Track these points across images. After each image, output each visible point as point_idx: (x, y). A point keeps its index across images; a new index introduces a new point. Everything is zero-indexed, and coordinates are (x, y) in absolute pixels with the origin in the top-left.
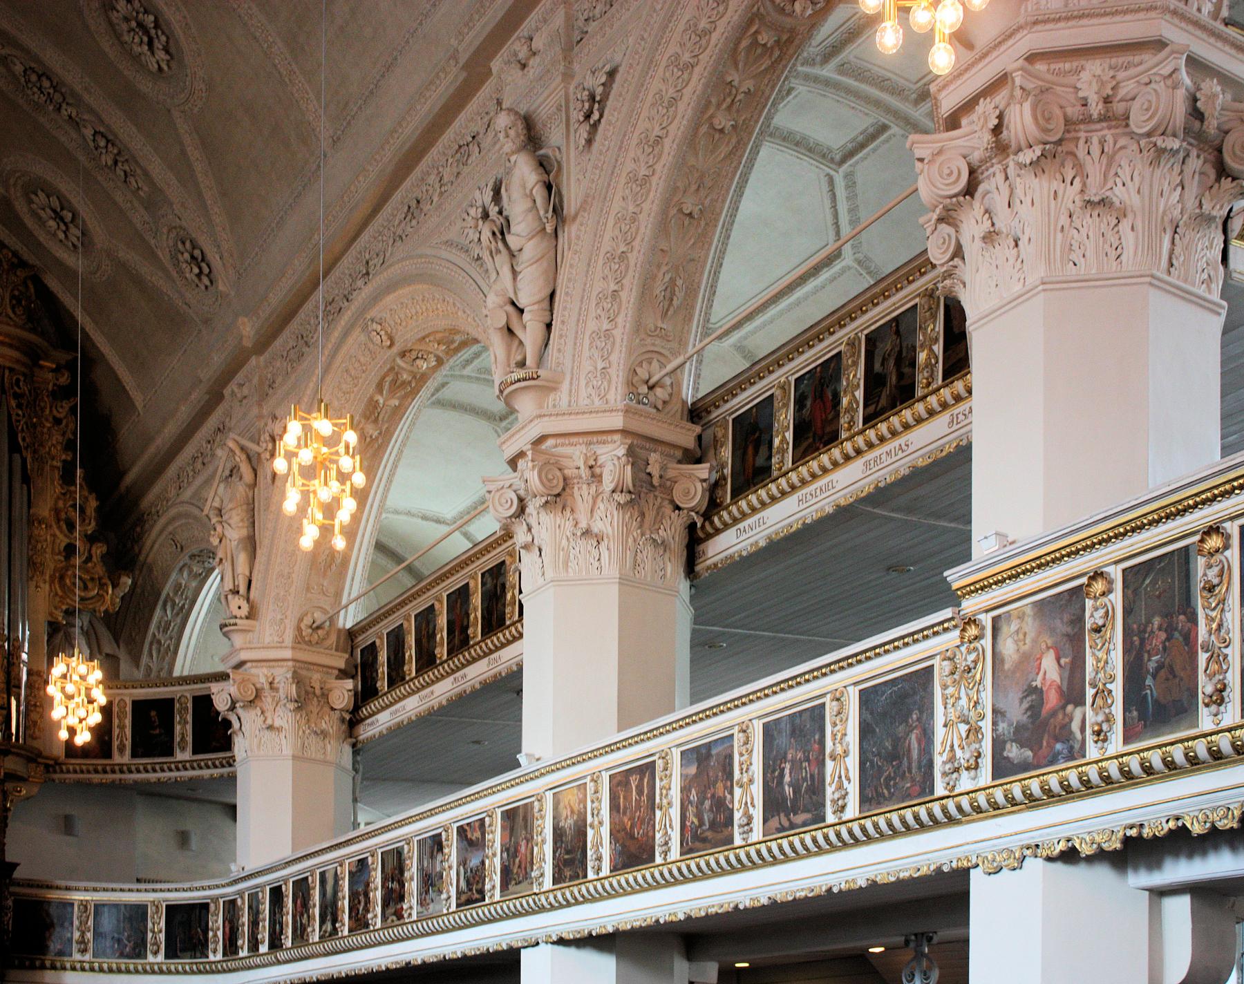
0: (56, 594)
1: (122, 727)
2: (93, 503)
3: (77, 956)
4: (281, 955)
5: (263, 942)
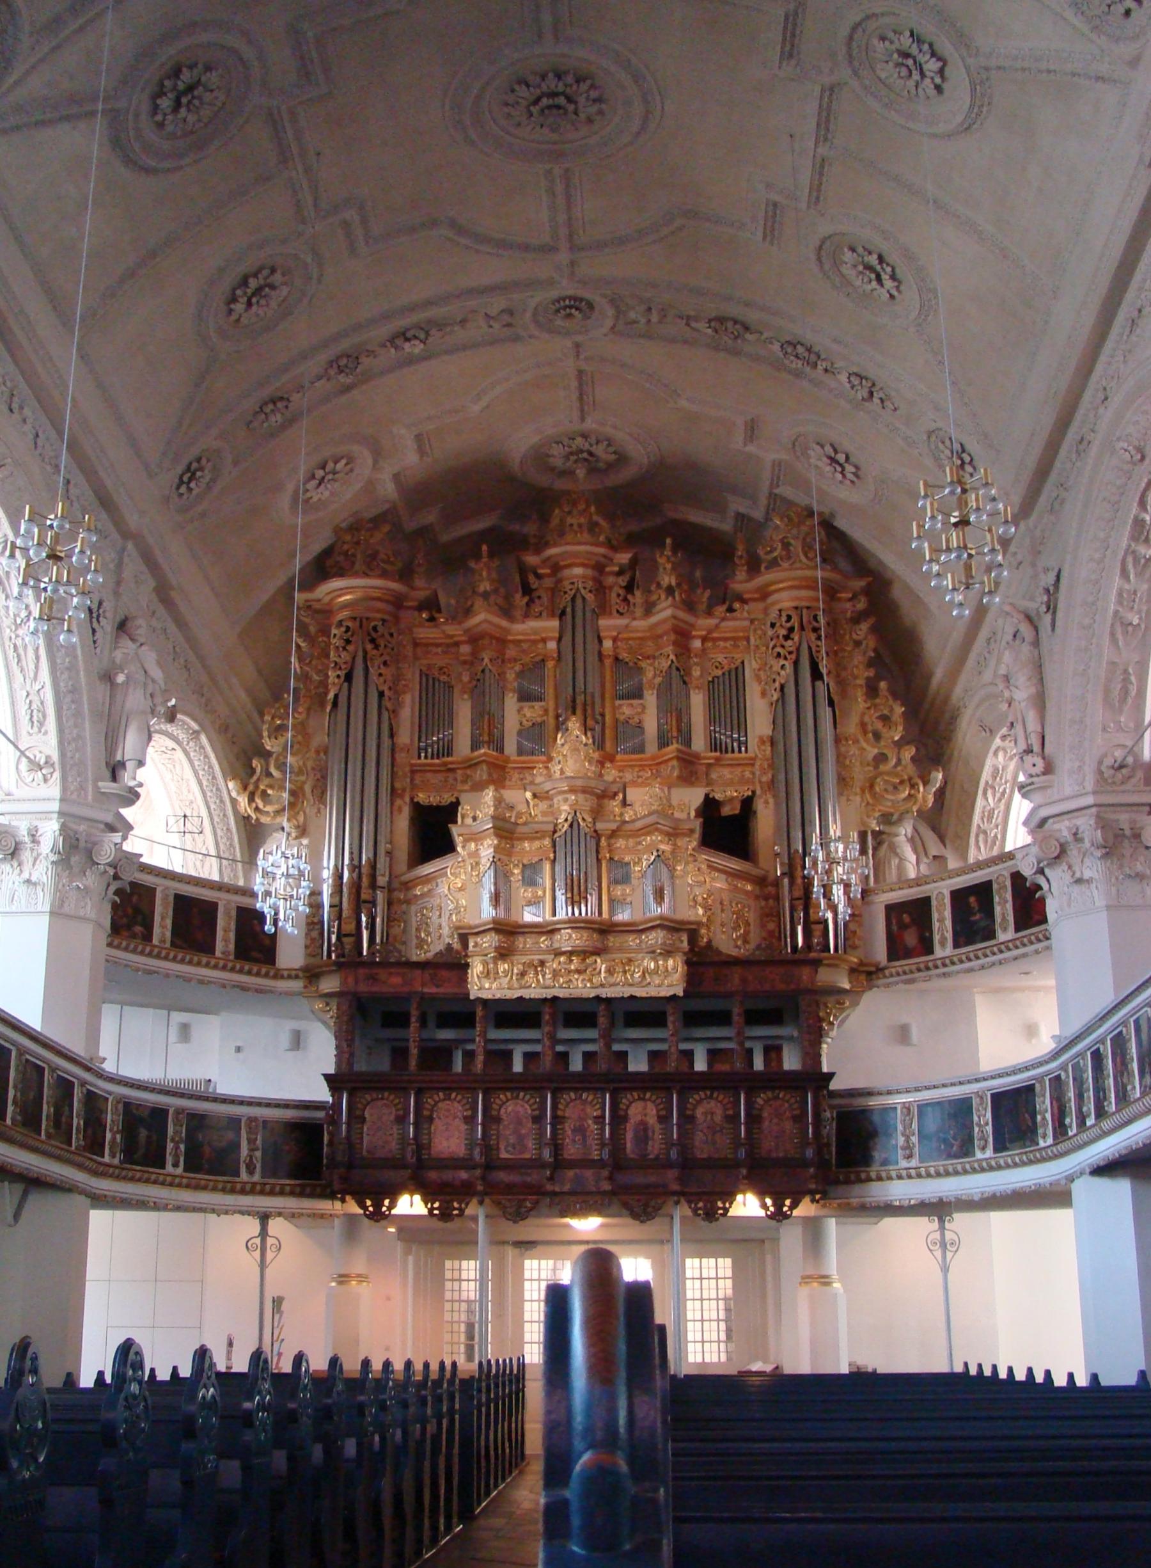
0: (868, 803)
1: (941, 920)
3: (904, 1164)
4: (1106, 1125)
5: (1089, 1115)
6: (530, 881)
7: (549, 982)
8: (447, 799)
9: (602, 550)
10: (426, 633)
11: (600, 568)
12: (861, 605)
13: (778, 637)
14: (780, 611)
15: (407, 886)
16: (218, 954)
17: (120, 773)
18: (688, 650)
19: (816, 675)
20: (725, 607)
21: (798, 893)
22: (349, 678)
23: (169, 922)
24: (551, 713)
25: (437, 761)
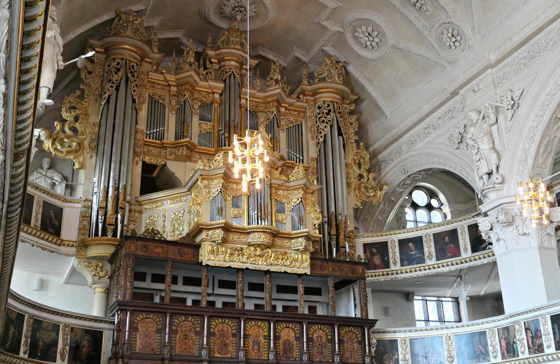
0: (357, 196)
1: (394, 253)
7: (245, 260)
10: (154, 76)
13: (323, 113)
14: (324, 102)
15: (140, 203)
16: (32, 225)
19: (340, 134)
21: (333, 232)
22: (117, 89)
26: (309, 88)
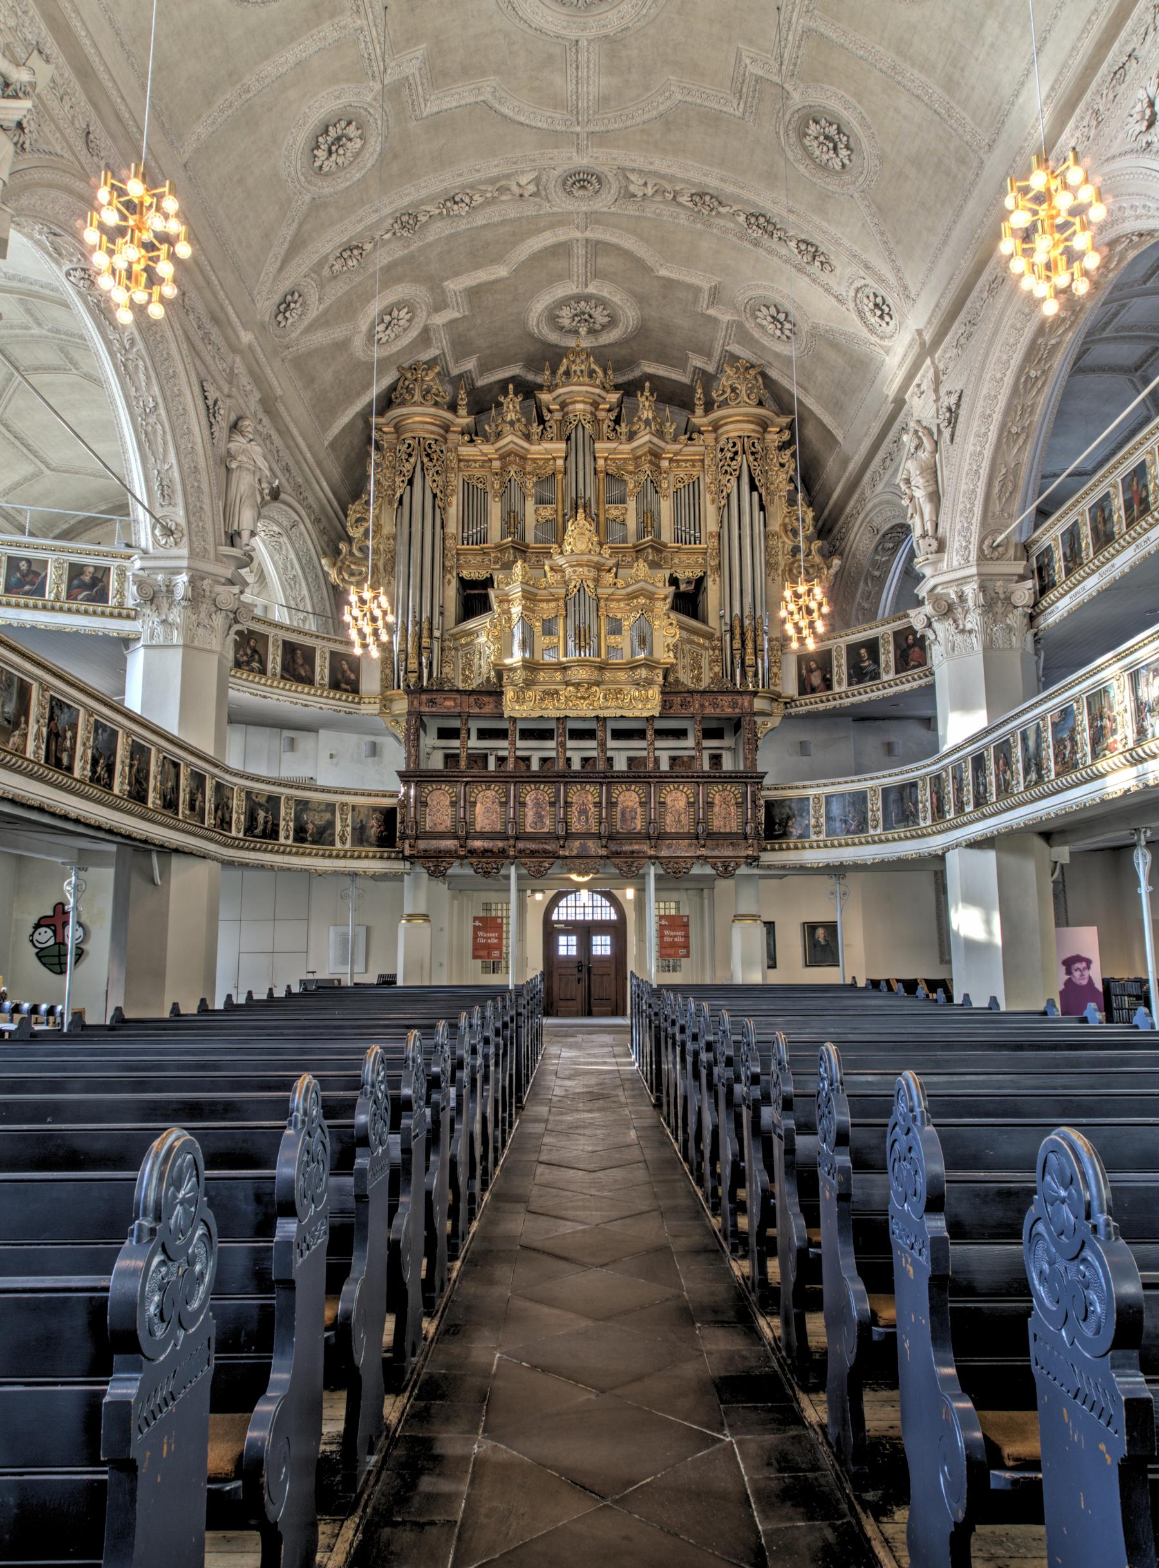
1: (839, 666)
2: (810, 514)
6: (548, 630)
8: (483, 575)
9: (597, 391)
10: (466, 451)
11: (595, 405)
12: (786, 436)
16: (317, 685)
17: (237, 540)
18: (659, 467)
19: (753, 487)
20: (687, 436)
22: (411, 482)
23: (279, 660)
24: (560, 513)
25: (475, 547)
26: (705, 420)
